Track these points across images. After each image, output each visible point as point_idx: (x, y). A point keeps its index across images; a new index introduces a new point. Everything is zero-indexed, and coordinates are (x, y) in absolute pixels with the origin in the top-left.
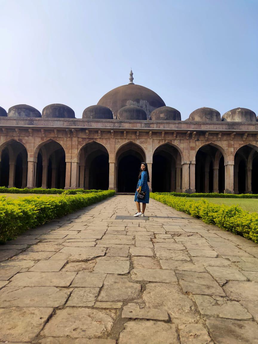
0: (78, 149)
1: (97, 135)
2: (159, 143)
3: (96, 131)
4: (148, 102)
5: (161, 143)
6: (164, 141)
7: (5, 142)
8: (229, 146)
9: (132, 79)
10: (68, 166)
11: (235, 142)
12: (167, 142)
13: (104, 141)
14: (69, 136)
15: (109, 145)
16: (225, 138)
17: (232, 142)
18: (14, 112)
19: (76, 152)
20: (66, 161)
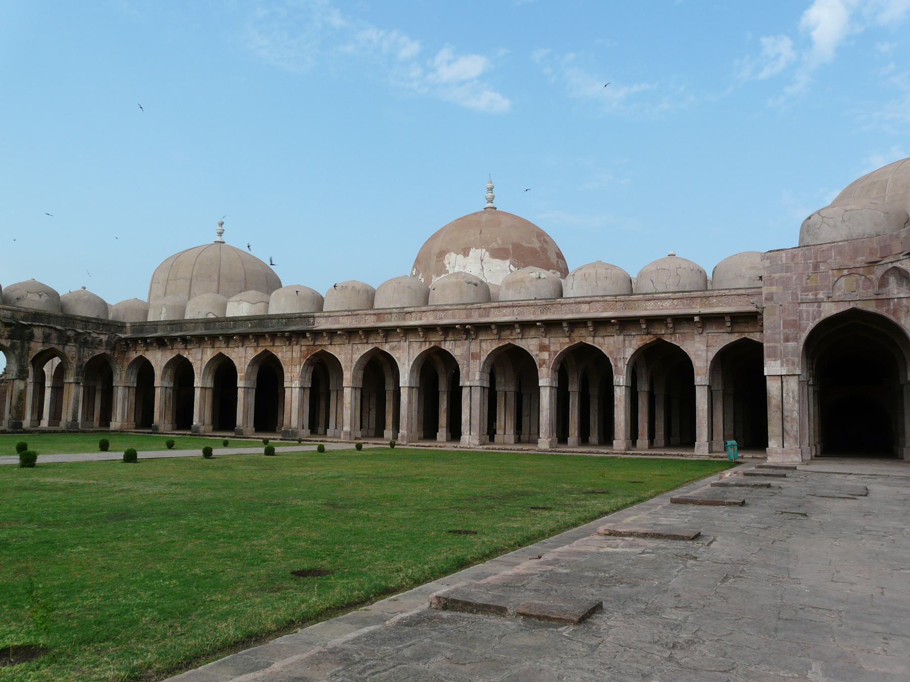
2: (420, 347)
5: (424, 349)
8: (543, 348)
10: (287, 392)
11: (553, 340)
13: (337, 349)
15: (343, 356)
16: (533, 333)
17: (546, 341)
19: (298, 369)
20: (286, 385)
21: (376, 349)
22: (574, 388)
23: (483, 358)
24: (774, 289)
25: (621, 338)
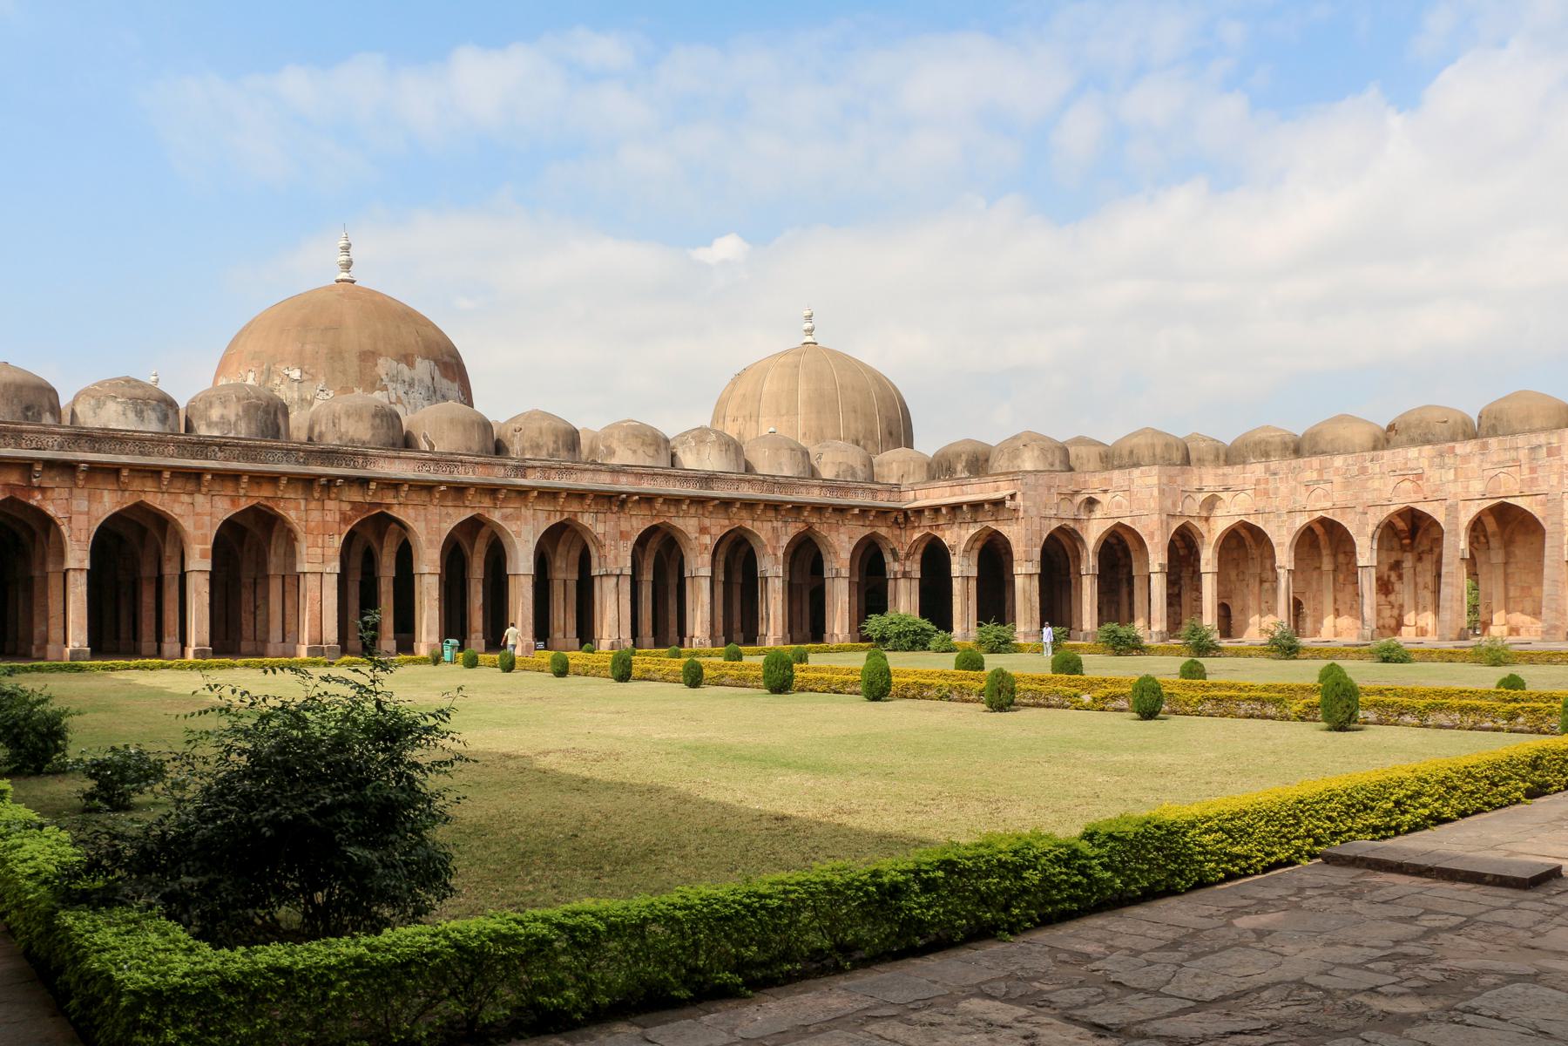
1: (392, 494)
2: (548, 518)
3: (394, 485)
5: (553, 521)
8: (703, 530)
12: (566, 516)
13: (411, 511)
14: (317, 495)
15: (423, 524)
16: (692, 511)
17: (707, 522)
18: (120, 408)
22: (647, 577)
23: (634, 538)
24: (1028, 504)
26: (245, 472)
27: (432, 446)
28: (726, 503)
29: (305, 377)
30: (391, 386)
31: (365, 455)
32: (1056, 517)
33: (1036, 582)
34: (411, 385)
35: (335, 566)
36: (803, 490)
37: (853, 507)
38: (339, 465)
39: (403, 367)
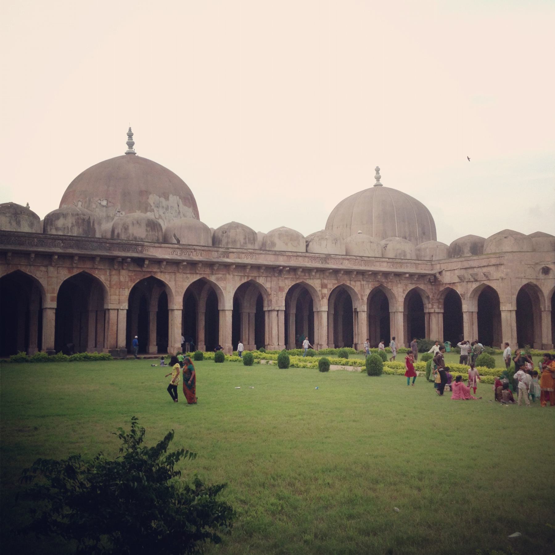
0: (129, 289)
2: (241, 280)
3: (158, 262)
4: (180, 198)
6: (246, 277)
7: (5, 274)
8: (324, 286)
9: (131, 144)
10: (113, 315)
11: (329, 281)
12: (250, 278)
16: (318, 275)
17: (325, 281)
18: (8, 219)
21: (204, 278)
22: (293, 311)
23: (286, 291)
24: (509, 270)
25: (365, 283)
26: (76, 254)
27: (178, 241)
28: (336, 272)
29: (109, 204)
30: (155, 209)
31: (143, 246)
32: (525, 278)
33: (514, 315)
34: (167, 209)
35: (126, 306)
36: (378, 264)
37: (405, 273)
38: (128, 251)
39: (162, 199)
